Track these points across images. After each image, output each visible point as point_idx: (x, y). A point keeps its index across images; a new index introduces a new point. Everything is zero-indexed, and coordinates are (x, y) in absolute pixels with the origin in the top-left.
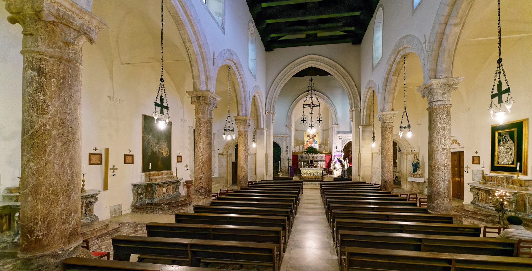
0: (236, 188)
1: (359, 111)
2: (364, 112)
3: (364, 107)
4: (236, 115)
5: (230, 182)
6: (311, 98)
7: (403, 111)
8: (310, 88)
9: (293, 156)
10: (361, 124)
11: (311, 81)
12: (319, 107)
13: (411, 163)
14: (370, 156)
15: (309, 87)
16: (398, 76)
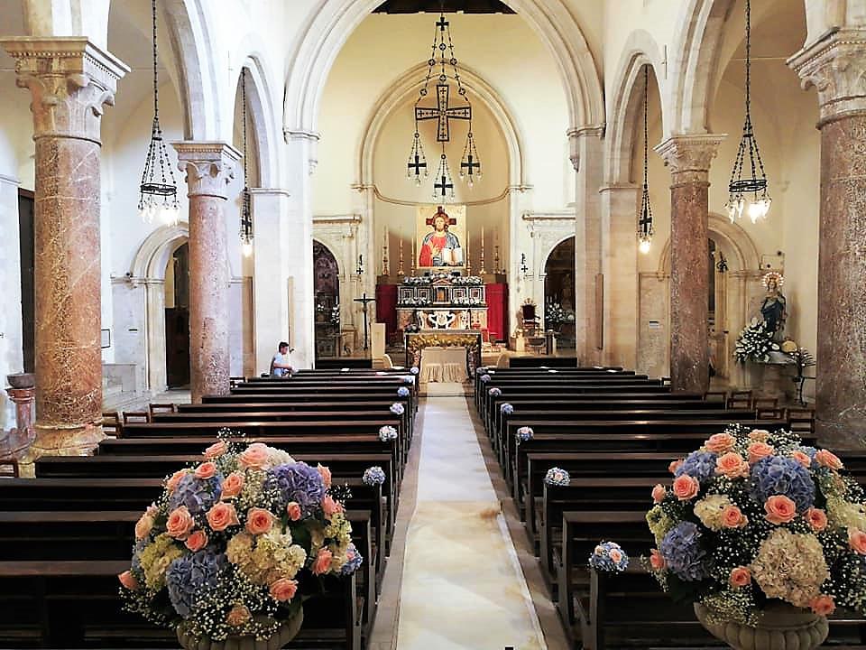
0: (184, 399)
2: (614, 140)
3: (616, 122)
4: (182, 139)
5: (160, 382)
6: (440, 88)
7: (742, 133)
9: (378, 288)
12: (470, 119)
13: (760, 307)
14: (634, 287)
15: (434, 47)
16: (725, 20)
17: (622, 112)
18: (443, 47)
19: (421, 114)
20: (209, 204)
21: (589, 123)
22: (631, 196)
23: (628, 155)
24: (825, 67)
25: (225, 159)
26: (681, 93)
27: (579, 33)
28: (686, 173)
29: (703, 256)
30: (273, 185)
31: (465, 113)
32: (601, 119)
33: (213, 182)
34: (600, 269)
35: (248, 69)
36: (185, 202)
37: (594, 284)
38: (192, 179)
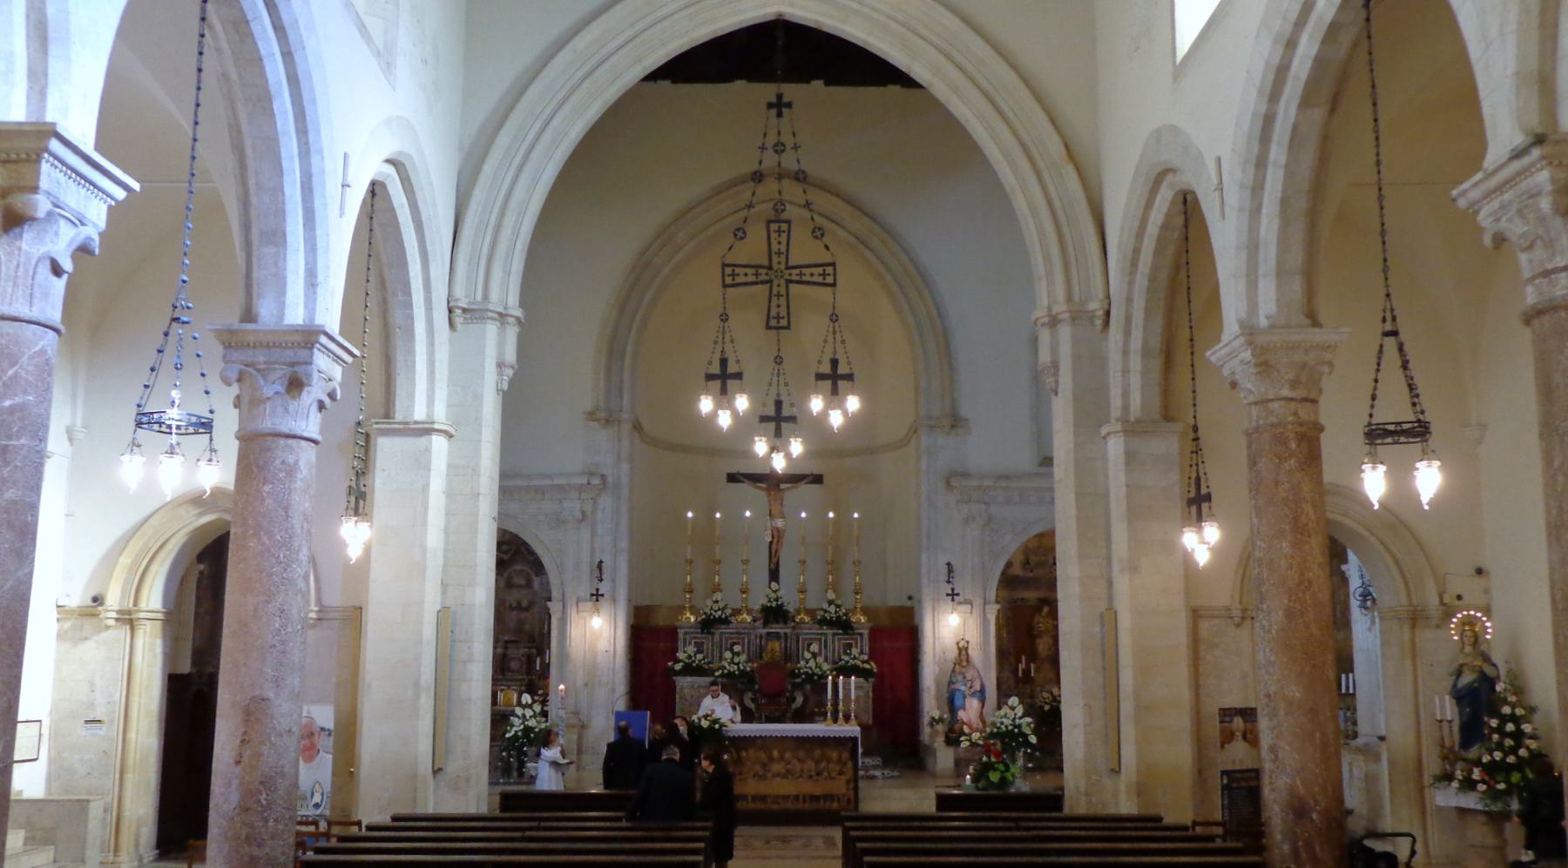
1: (1099, 322)
2: (1127, 332)
3: (1129, 300)
4: (233, 321)
6: (774, 226)
7: (1379, 328)
8: (770, 160)
10: (1116, 410)
11: (774, 112)
12: (834, 285)
14: (1181, 638)
17: (1141, 281)
18: (779, 148)
19: (733, 275)
20: (284, 453)
21: (1076, 297)
22: (1168, 445)
23: (1156, 364)
24: (1526, 206)
25: (321, 361)
26: (1252, 248)
27: (1049, 127)
28: (1275, 405)
29: (1318, 571)
30: (419, 414)
31: (824, 275)
32: (1101, 294)
33: (291, 409)
34: (1110, 598)
35: (383, 185)
36: (229, 448)
37: (1097, 629)
38: (247, 404)
